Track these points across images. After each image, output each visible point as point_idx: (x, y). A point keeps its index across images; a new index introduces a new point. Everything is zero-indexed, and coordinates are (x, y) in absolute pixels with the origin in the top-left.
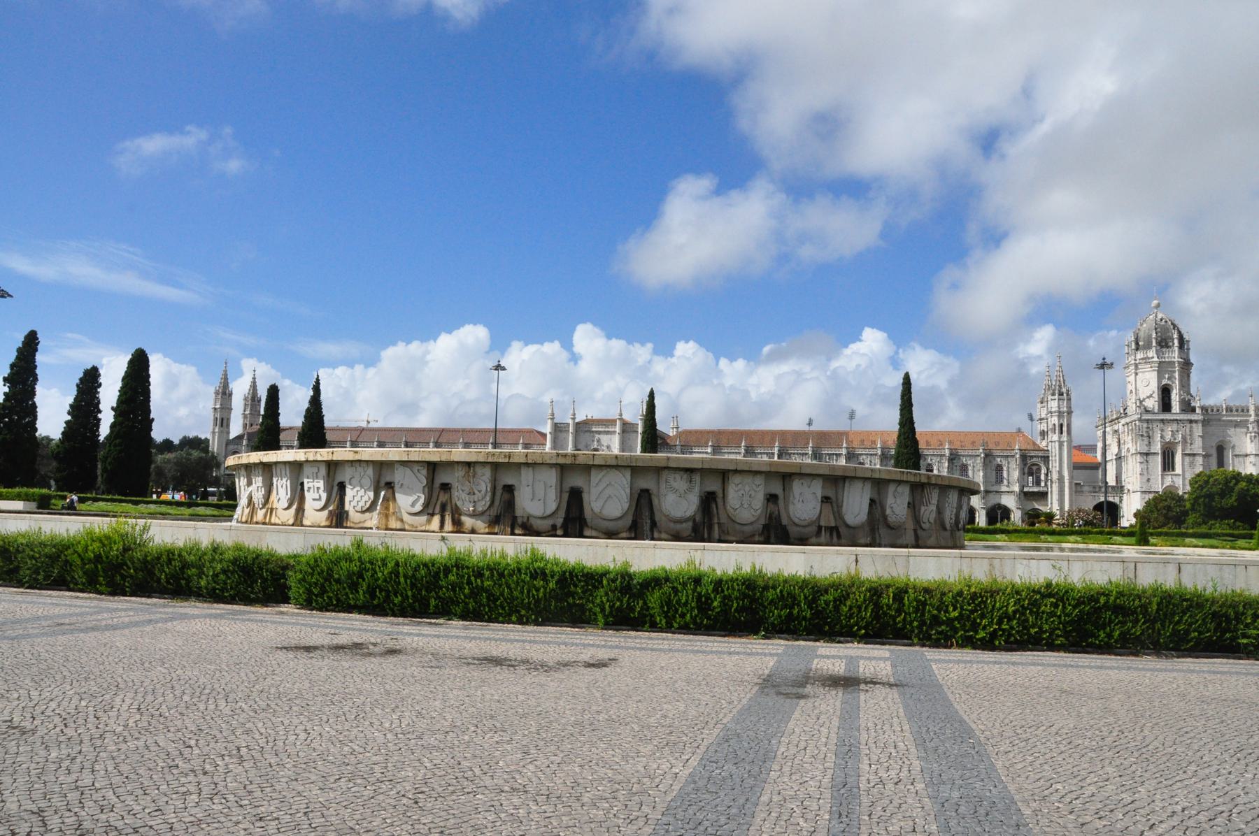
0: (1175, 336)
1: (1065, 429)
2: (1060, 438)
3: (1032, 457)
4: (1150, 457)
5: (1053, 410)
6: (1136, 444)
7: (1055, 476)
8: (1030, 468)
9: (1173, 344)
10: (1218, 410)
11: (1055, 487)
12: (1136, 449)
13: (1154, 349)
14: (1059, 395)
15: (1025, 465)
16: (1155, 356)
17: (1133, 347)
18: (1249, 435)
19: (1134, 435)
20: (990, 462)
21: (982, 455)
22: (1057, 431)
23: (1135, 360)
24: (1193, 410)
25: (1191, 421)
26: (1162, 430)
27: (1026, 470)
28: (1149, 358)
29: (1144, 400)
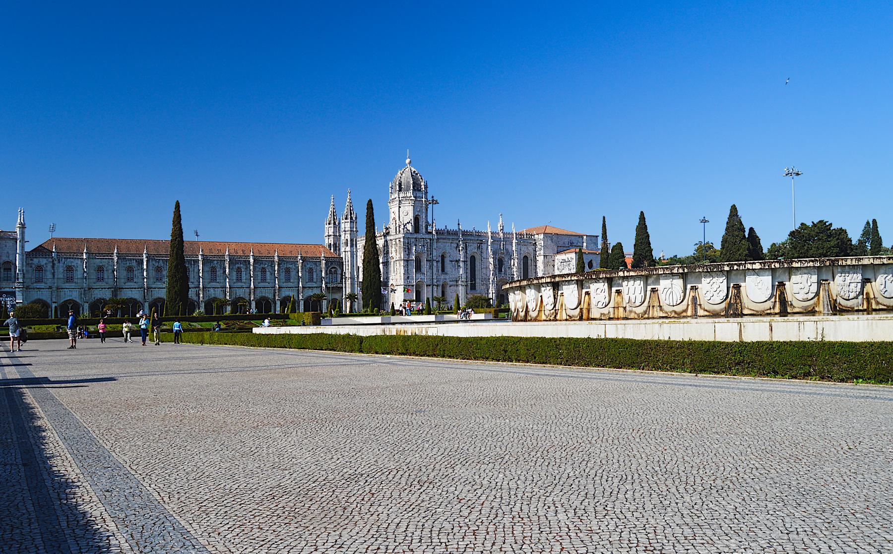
4: (410, 261)
6: (400, 254)
8: (330, 270)
10: (443, 233)
14: (351, 219)
16: (412, 196)
17: (398, 189)
19: (398, 248)
22: (349, 245)
23: (399, 198)
24: (431, 233)
27: (328, 272)
29: (406, 224)
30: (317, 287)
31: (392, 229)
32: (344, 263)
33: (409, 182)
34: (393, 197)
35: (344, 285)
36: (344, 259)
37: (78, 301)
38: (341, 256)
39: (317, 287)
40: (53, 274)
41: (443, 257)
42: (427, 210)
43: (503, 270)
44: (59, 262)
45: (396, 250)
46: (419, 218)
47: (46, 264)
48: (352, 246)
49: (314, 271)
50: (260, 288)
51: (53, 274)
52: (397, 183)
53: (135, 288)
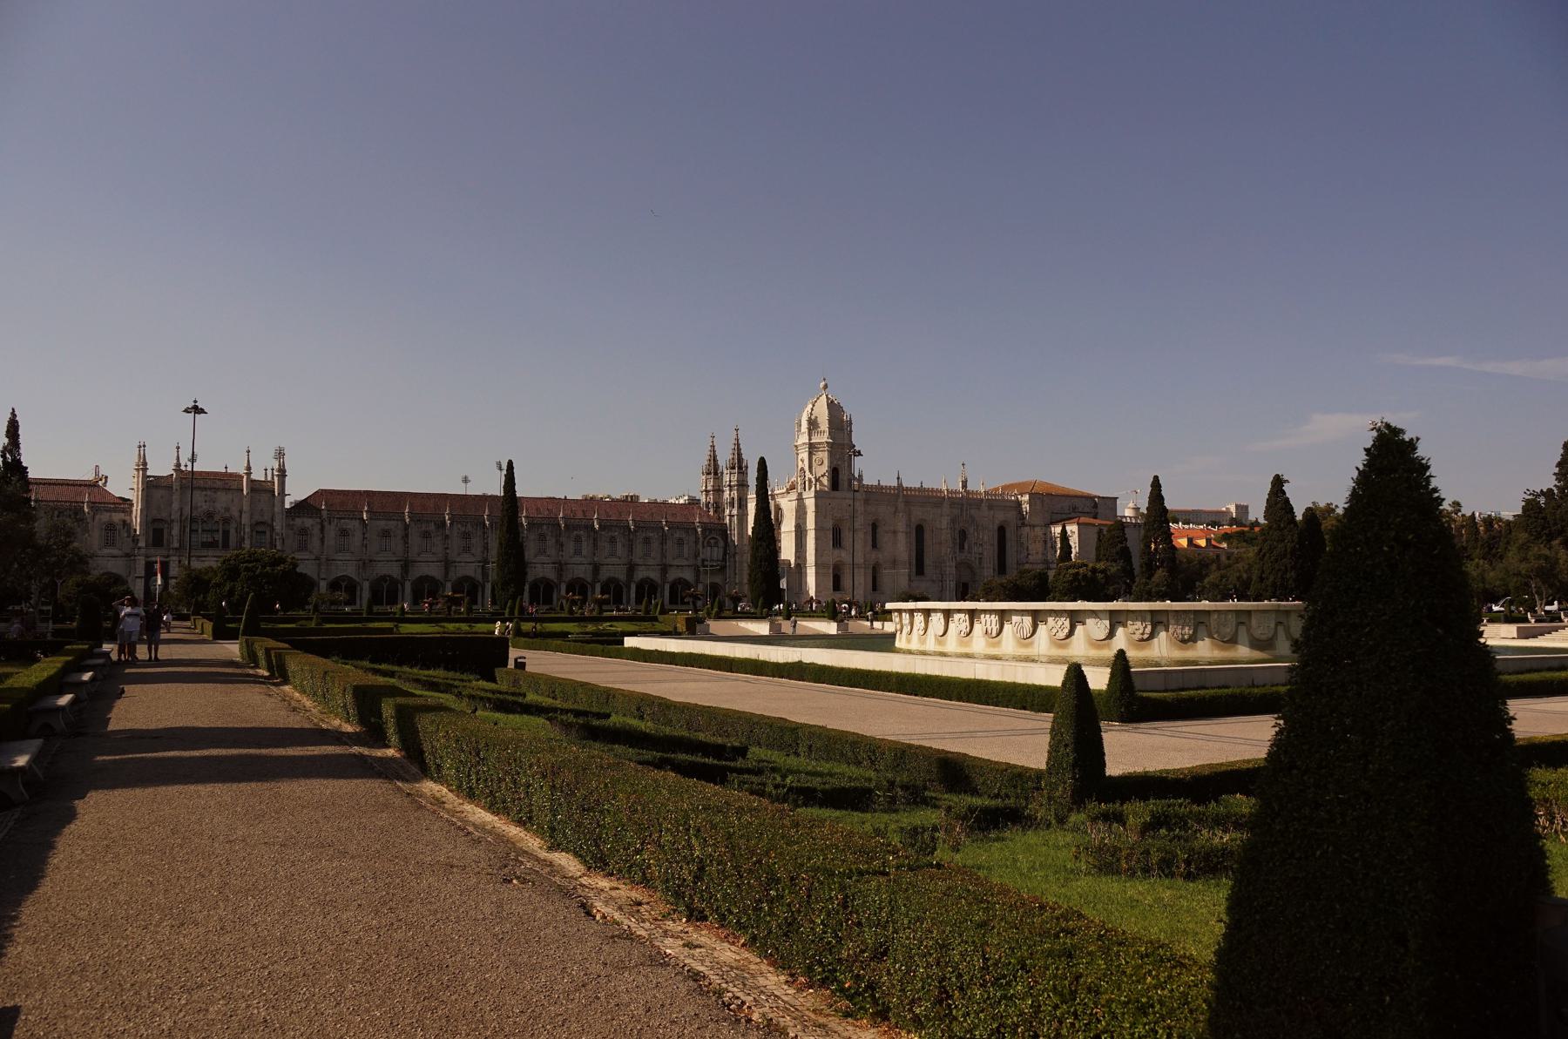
3: (711, 531)
8: (708, 542)
15: (704, 538)
20: (672, 535)
22: (736, 505)
27: (705, 544)
37: (354, 577)
40: (322, 540)
41: (874, 527)
43: (966, 547)
44: (330, 523)
47: (312, 526)
49: (685, 542)
50: (607, 565)
51: (322, 540)
53: (433, 562)
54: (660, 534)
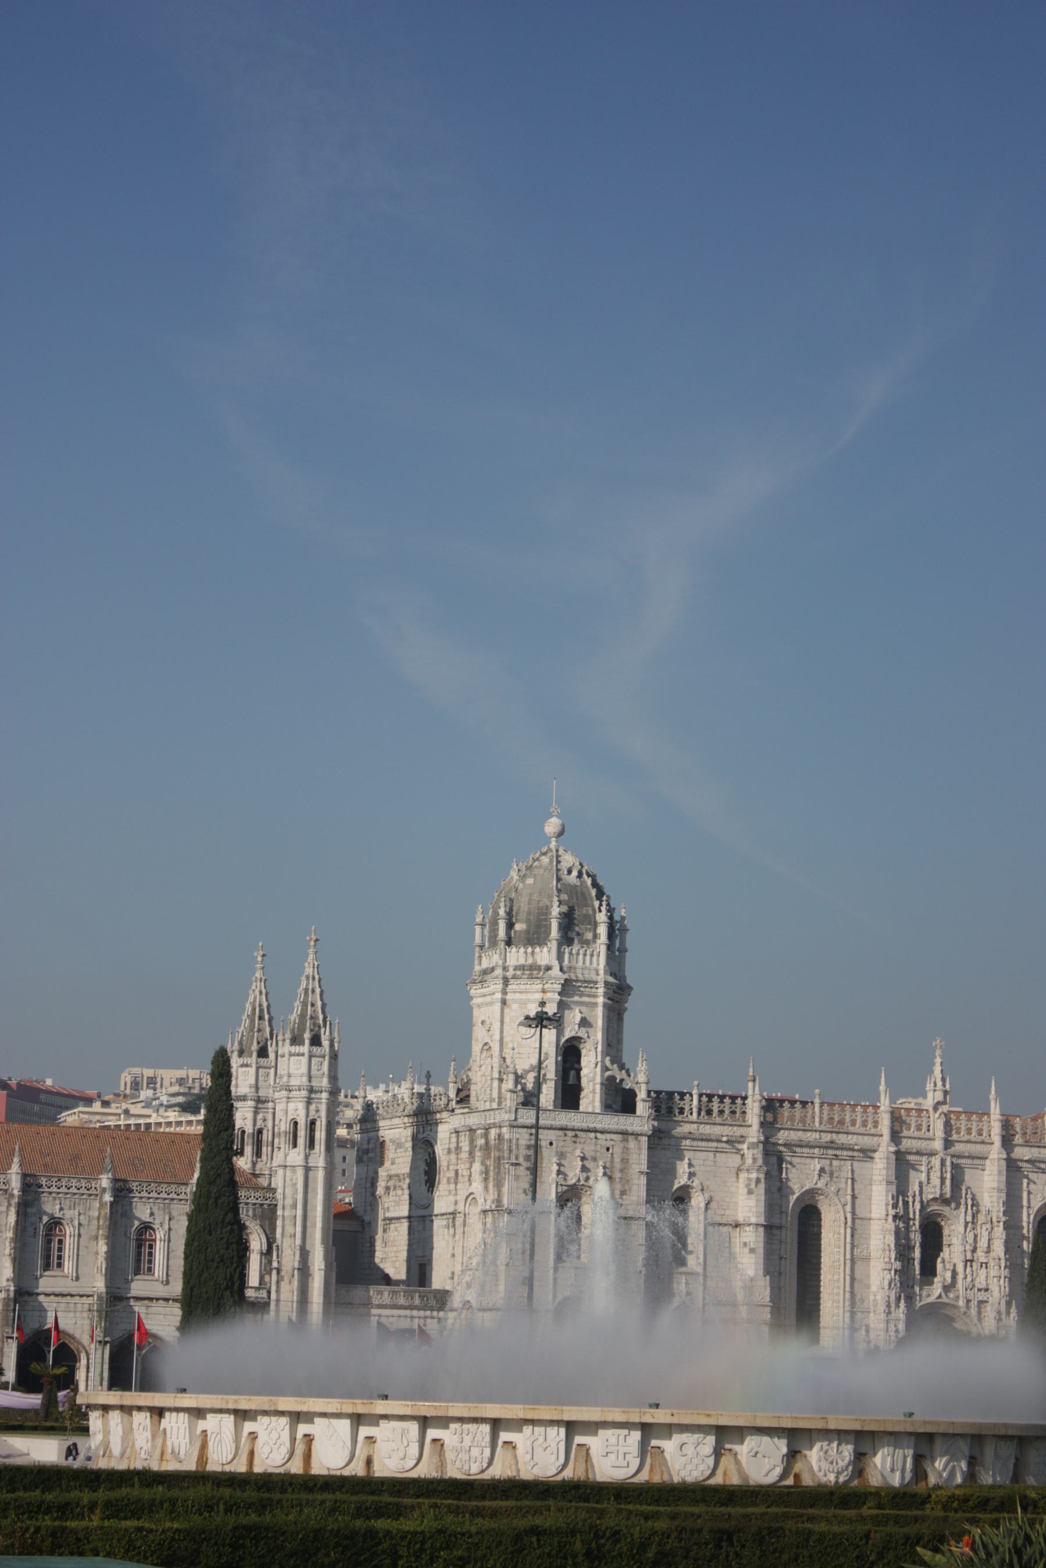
0: (602, 917)
1: (320, 1135)
2: (307, 1157)
5: (295, 1082)
6: (499, 1186)
7: (289, 1259)
9: (596, 936)
11: (289, 1291)
12: (499, 1201)
13: (553, 945)
17: (502, 933)
18: (743, 1176)
19: (490, 1163)
21: (108, 1198)
22: (301, 1141)
25: (624, 1133)
26: (561, 1155)
28: (539, 968)
30: (166, 1300)
31: (479, 1085)
32: (279, 1212)
33: (544, 914)
34: (486, 964)
35: (273, 1296)
36: (279, 1195)
38: (273, 1185)
39: (166, 1300)
42: (620, 1018)
45: (487, 1173)
46: (584, 1052)
48: (311, 1143)
52: (502, 912)
54: (96, 1214)
